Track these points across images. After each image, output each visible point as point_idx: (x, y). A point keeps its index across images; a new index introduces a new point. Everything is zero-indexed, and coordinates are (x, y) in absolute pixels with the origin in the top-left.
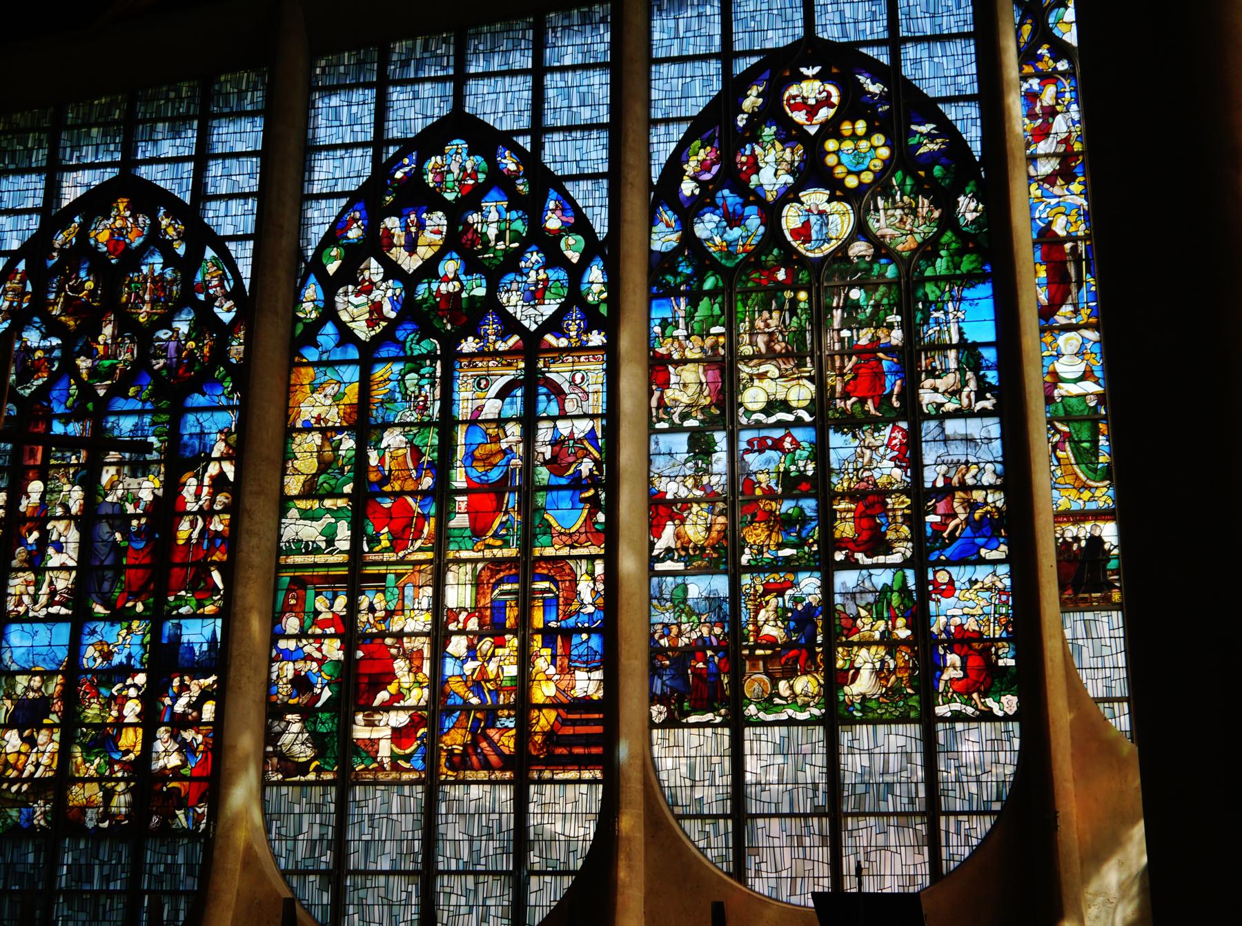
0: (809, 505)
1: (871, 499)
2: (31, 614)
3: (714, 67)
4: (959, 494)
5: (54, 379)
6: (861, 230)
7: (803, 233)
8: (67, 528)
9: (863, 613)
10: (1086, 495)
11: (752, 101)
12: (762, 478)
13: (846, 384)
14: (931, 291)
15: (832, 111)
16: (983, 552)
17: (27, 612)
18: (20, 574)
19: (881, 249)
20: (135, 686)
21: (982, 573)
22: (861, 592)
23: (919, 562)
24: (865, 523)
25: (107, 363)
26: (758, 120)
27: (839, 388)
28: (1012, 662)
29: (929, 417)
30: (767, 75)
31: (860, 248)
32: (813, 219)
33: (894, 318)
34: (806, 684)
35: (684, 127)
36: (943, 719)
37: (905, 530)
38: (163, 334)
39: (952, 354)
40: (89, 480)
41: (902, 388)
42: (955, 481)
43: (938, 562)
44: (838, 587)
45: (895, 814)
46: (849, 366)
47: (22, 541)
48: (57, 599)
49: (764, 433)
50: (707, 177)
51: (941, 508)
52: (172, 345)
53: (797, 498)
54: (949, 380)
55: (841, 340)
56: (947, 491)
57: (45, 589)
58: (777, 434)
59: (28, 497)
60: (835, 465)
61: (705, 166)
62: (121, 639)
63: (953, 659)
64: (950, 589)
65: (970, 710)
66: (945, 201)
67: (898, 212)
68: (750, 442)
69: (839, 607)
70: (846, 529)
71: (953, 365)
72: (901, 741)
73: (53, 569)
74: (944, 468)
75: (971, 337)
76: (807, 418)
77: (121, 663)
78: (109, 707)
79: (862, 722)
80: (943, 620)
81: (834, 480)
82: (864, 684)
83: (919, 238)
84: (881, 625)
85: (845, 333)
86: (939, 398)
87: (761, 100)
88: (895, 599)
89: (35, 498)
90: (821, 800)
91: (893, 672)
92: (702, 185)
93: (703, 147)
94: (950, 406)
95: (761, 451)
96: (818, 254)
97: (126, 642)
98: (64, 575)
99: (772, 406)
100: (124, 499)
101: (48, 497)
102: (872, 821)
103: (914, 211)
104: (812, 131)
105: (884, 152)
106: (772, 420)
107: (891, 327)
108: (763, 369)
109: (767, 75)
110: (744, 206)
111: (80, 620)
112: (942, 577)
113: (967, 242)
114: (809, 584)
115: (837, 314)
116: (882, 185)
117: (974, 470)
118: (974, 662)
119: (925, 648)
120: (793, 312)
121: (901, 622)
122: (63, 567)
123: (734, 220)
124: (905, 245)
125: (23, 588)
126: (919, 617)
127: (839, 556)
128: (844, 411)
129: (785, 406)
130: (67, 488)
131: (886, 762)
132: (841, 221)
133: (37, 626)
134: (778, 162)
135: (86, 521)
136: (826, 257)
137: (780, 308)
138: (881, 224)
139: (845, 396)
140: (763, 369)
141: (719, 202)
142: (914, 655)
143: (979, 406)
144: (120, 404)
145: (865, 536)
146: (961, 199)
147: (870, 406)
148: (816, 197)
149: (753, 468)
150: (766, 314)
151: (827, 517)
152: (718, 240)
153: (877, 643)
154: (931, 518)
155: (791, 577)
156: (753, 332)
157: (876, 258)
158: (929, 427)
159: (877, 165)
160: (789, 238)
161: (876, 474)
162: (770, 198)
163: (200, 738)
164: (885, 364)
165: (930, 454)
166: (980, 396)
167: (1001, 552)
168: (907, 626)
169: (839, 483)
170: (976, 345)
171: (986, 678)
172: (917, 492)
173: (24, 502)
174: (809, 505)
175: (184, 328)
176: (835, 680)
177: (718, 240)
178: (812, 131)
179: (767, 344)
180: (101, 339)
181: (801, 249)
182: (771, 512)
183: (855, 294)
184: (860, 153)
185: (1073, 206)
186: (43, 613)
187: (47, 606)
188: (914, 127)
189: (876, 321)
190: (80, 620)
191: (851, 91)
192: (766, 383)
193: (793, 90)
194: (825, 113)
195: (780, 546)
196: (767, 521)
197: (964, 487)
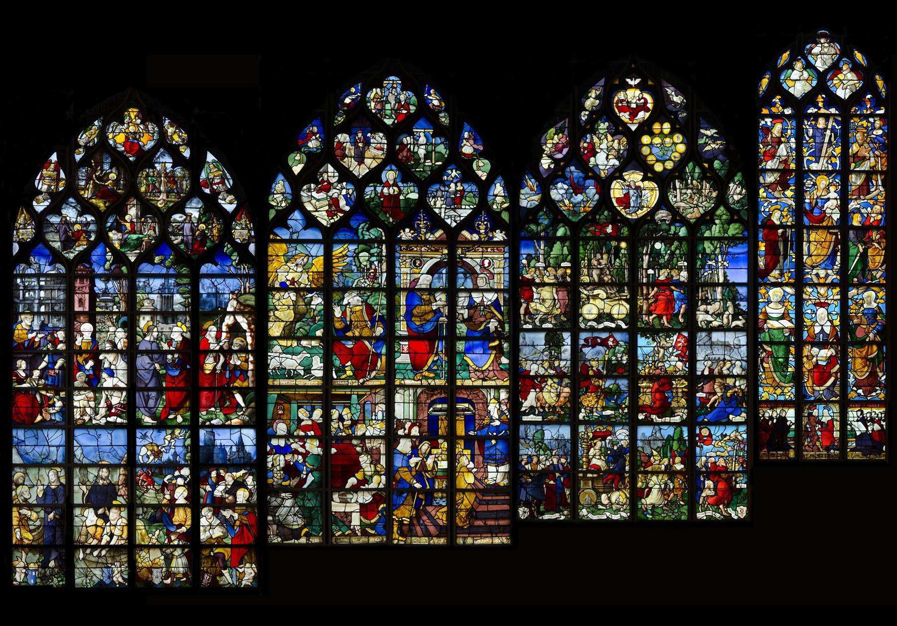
1: (664, 380)
2: (94, 422)
5: (92, 246)
8: (116, 359)
9: (655, 453)
13: (650, 305)
17: (91, 420)
18: (82, 392)
20: (181, 476)
22: (654, 440)
23: (691, 422)
24: (658, 396)
25: (134, 237)
29: (702, 330)
37: (683, 402)
38: (177, 217)
40: (131, 327)
41: (686, 310)
47: (80, 368)
48: (113, 411)
51: (707, 388)
52: (187, 226)
54: (715, 307)
55: (648, 276)
57: (103, 404)
59: (82, 335)
62: (167, 443)
63: (709, 483)
67: (689, 191)
69: (640, 449)
73: (108, 389)
74: (710, 363)
77: (169, 459)
78: (163, 492)
80: (704, 459)
84: (666, 461)
88: (675, 445)
89: (87, 336)
91: (671, 491)
97: (172, 444)
98: (116, 394)
100: (159, 339)
101: (97, 335)
111: (133, 426)
112: (705, 432)
116: (678, 172)
121: (678, 459)
122: (115, 388)
125: (85, 403)
126: (689, 457)
130: (112, 329)
133: (100, 432)
135: (131, 353)
139: (649, 313)
142: (686, 480)
144: (145, 268)
153: (663, 473)
154: (699, 395)
157: (673, 222)
159: (676, 156)
163: (236, 516)
165: (701, 354)
168: (682, 462)
172: (693, 378)
173: (79, 339)
175: (195, 214)
180: (127, 218)
186: (103, 421)
187: (106, 416)
188: (702, 131)
190: (133, 426)
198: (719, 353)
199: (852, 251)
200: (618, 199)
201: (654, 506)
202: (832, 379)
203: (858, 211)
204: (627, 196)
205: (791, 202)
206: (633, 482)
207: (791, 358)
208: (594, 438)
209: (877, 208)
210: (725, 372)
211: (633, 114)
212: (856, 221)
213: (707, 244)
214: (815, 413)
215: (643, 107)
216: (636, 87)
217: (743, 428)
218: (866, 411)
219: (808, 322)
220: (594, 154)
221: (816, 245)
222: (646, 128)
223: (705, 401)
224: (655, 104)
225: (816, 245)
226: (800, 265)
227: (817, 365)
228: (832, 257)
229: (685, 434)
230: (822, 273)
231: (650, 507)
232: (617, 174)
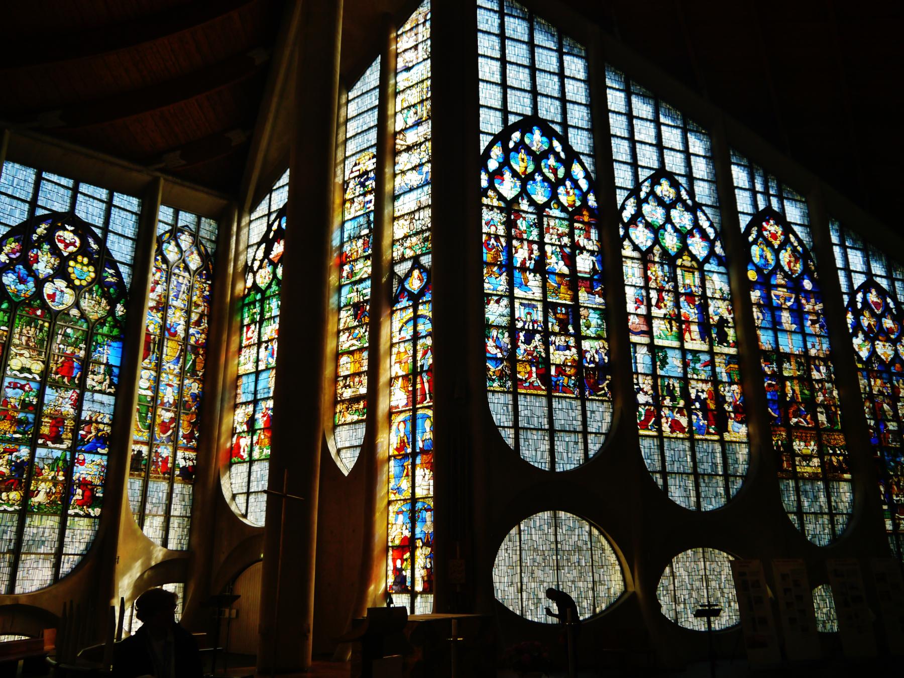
0: (31, 417)
1: (58, 420)
3: (26, 207)
4: (94, 425)
6: (77, 305)
7: (52, 297)
9: (46, 467)
10: (140, 434)
11: (41, 230)
12: (12, 400)
13: (58, 368)
14: (100, 339)
15: (75, 249)
16: (99, 450)
19: (83, 316)
21: (97, 458)
23: (73, 450)
24: (54, 429)
26: (42, 239)
27: (54, 369)
28: (101, 495)
29: (89, 390)
30: (50, 221)
31: (74, 312)
32: (58, 293)
33: (83, 346)
34: (15, 495)
35: (8, 229)
36: (71, 515)
37: (70, 435)
39: (103, 367)
41: (81, 375)
42: (94, 419)
43: (81, 451)
44: (37, 455)
45: (43, 554)
46: (60, 360)
49: (17, 381)
50: (13, 256)
51: (86, 428)
53: (27, 413)
54: (99, 377)
55: (59, 349)
56: (90, 423)
58: (23, 382)
60: (46, 402)
61: (13, 251)
63: (79, 491)
64: (83, 463)
65: (82, 513)
66: (112, 303)
67: (93, 302)
68: (10, 383)
70: (45, 430)
71: (102, 372)
72: (52, 523)
75: (111, 362)
76: (38, 378)
79: (36, 514)
80: (78, 475)
81: (45, 408)
82: (41, 498)
83: (99, 316)
84: (53, 474)
85: (62, 346)
86: (94, 384)
87: (45, 232)
88: (61, 463)
90: (12, 547)
91: (53, 494)
92: (10, 259)
93: (14, 242)
94: (98, 388)
95: (14, 388)
96: (57, 309)
99: (23, 370)
102: (33, 556)
103: (99, 304)
104: (65, 254)
105: (93, 275)
106: (22, 376)
107: (81, 349)
108: (22, 352)
109: (50, 221)
110: (28, 276)
112: (81, 457)
113: (117, 323)
114: (24, 452)
115: (60, 337)
117: (102, 416)
118: (87, 493)
119: (69, 485)
120: (41, 330)
121: (61, 473)
123: (22, 281)
124: (93, 317)
126: (69, 471)
127: (40, 441)
128: (54, 379)
129: (29, 371)
131: (44, 532)
132: (69, 298)
134: (48, 262)
136: (60, 311)
137: (36, 327)
138: (85, 304)
139: (56, 373)
140: (22, 352)
141: (17, 270)
142: (64, 488)
143: (108, 390)
145: (53, 435)
146: (118, 305)
147: (66, 380)
148: (61, 284)
149: (9, 395)
150: (28, 328)
151: (38, 423)
152: (13, 287)
154: (81, 432)
155: (17, 447)
156: (21, 334)
158: (88, 395)
159: (89, 279)
160: (46, 297)
161: (63, 409)
162: (41, 276)
164: (75, 364)
166: (110, 387)
167: (105, 451)
168: (63, 475)
169: (46, 410)
170: (112, 366)
171: (90, 500)
172: (78, 421)
174: (31, 417)
176: (28, 494)
177: (13, 287)
178: (65, 254)
179: (27, 341)
181: (50, 304)
182: (14, 417)
183: (69, 331)
184: (81, 271)
185: (157, 322)
189: (75, 344)
191: (85, 244)
192: (22, 358)
193: (60, 233)
194: (72, 249)
195: (15, 432)
196: (11, 420)
197: (97, 422)
198: (97, 407)
199: (188, 357)
200: (49, 296)
201: (40, 503)
202: (171, 431)
203: (193, 335)
204: (54, 294)
205: (160, 321)
206: (28, 484)
207: (150, 415)
208: (4, 452)
209: (203, 336)
210: (99, 420)
211: (67, 246)
212: (192, 341)
213: (99, 337)
214: (159, 450)
215: (73, 244)
216: (71, 231)
217: (105, 458)
218: (187, 453)
219: (161, 394)
220: (38, 262)
221: (171, 349)
222: (73, 256)
223: (84, 437)
224: (81, 244)
225: (171, 349)
226: (160, 359)
227: (163, 422)
228: (178, 358)
229: (68, 458)
230: (172, 367)
231: (37, 504)
232: (50, 279)
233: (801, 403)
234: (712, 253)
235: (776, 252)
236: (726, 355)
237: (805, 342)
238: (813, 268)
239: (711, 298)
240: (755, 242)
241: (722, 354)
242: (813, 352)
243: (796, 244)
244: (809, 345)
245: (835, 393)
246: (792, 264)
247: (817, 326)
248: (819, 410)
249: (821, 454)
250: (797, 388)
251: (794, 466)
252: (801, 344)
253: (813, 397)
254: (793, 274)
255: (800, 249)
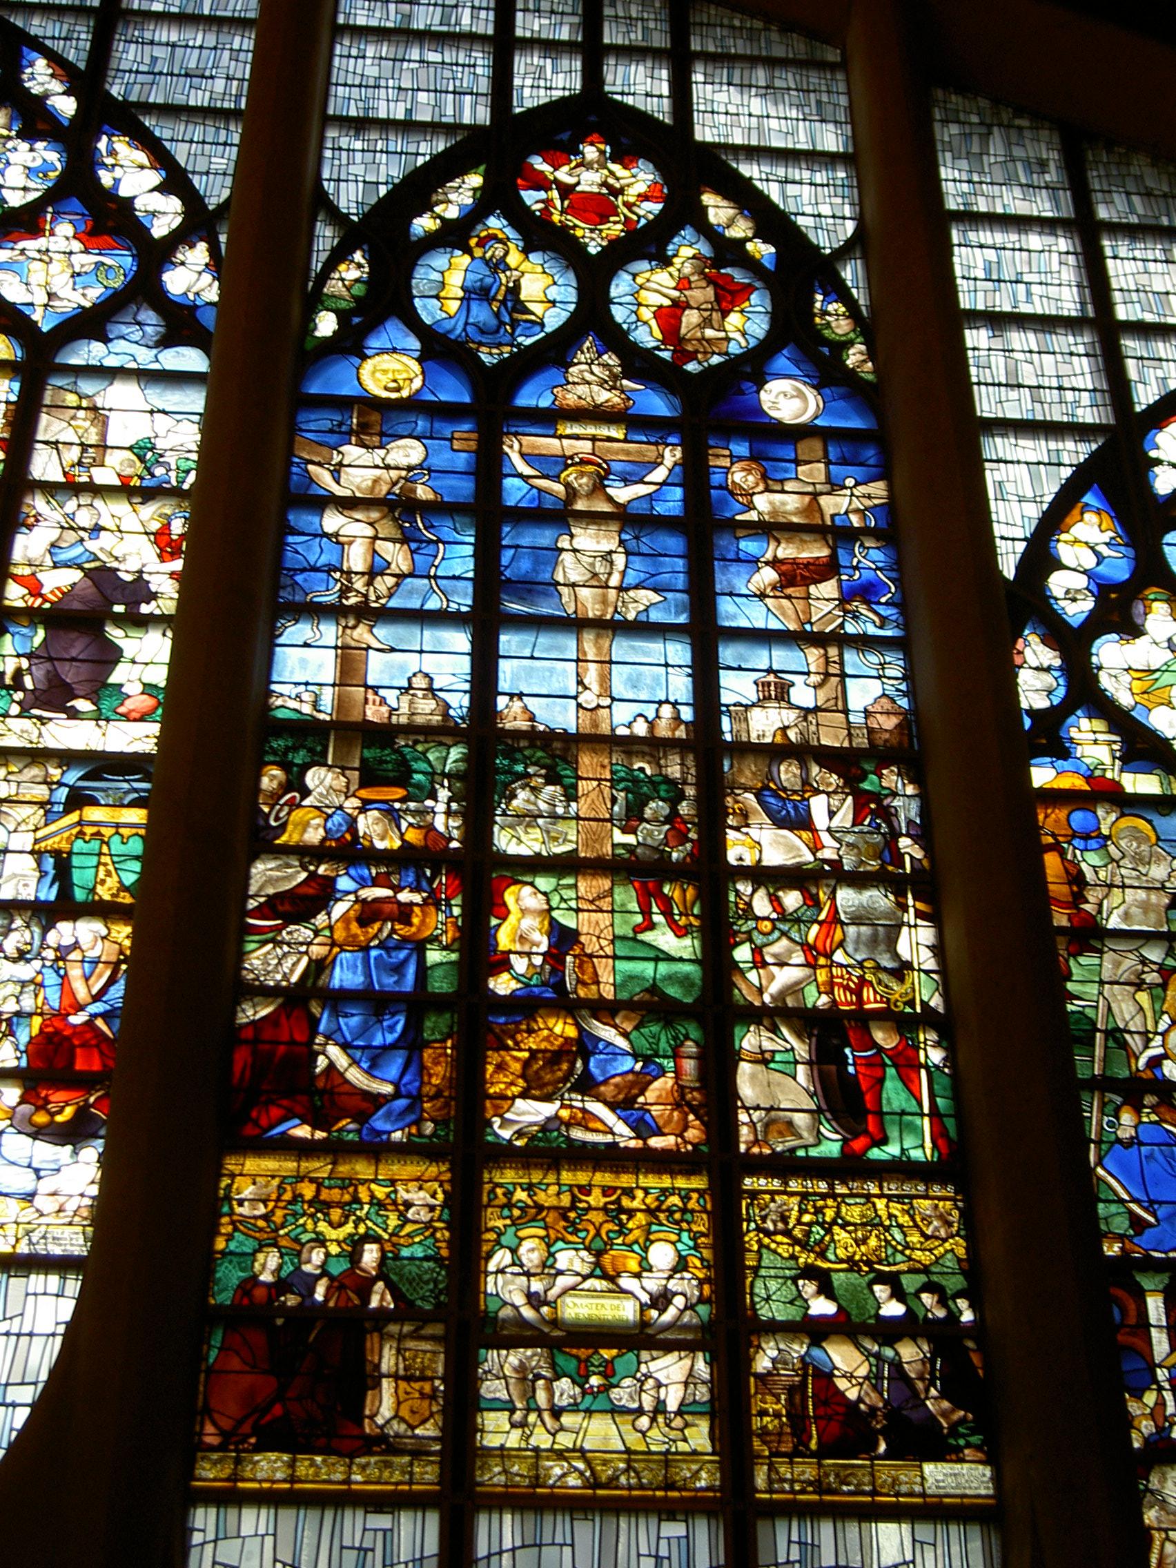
233: (605, 1010)
234: (144, 289)
235: (594, 277)
236: (67, 758)
237: (705, 676)
238: (842, 327)
239: (49, 489)
240: (454, 236)
241: (36, 755)
242: (765, 724)
243: (740, 229)
244: (736, 687)
245: (916, 942)
246: (691, 318)
247: (828, 589)
248: (750, 1040)
249: (726, 1330)
250: (594, 929)
251: (462, 1405)
252: (681, 686)
253: (717, 963)
254: (684, 355)
255: (762, 250)
